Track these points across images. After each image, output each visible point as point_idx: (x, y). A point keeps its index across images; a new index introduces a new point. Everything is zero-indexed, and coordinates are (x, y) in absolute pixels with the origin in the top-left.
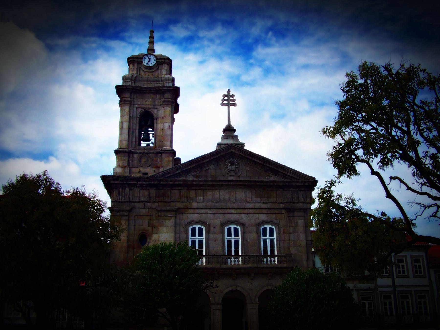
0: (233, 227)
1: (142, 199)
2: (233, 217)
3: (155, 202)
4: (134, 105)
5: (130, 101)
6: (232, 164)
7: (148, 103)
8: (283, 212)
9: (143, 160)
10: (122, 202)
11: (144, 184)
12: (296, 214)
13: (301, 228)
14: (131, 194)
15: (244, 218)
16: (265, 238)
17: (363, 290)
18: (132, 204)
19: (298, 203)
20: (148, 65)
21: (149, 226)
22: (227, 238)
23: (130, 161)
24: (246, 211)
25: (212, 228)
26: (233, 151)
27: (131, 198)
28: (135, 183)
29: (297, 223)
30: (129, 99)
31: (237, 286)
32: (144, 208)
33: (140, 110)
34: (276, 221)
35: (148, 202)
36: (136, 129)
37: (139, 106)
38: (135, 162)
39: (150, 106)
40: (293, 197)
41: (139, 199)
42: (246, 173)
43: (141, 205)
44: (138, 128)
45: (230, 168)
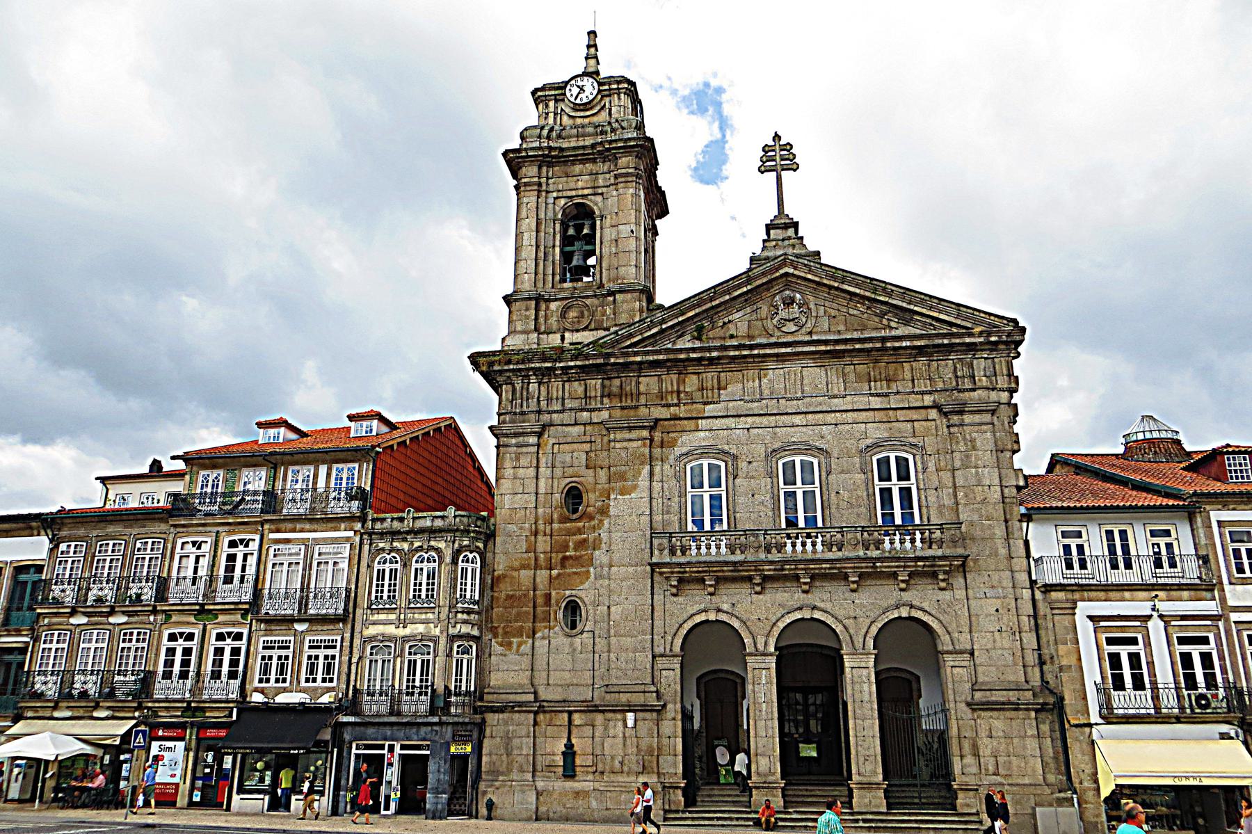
0: (798, 459)
1: (569, 404)
2: (797, 435)
3: (600, 410)
4: (548, 192)
5: (540, 184)
6: (789, 302)
7: (580, 184)
8: (933, 414)
9: (572, 314)
10: (523, 413)
11: (571, 368)
12: (968, 418)
13: (985, 455)
14: (544, 393)
15: (827, 437)
16: (885, 484)
17: (1184, 618)
18: (545, 418)
19: (974, 390)
20: (578, 101)
21: (587, 467)
22: (783, 488)
23: (542, 320)
24: (831, 418)
25: (743, 465)
26: (791, 271)
27: (543, 403)
28: (549, 365)
29: (973, 441)
30: (536, 179)
31: (814, 608)
32: (576, 424)
33: (563, 202)
34: (914, 441)
35: (582, 410)
36: (554, 246)
37: (560, 194)
38: (553, 321)
39: (586, 192)
40: (957, 377)
41: (563, 404)
42: (825, 321)
43: (567, 417)
44: (558, 243)
45: (783, 314)
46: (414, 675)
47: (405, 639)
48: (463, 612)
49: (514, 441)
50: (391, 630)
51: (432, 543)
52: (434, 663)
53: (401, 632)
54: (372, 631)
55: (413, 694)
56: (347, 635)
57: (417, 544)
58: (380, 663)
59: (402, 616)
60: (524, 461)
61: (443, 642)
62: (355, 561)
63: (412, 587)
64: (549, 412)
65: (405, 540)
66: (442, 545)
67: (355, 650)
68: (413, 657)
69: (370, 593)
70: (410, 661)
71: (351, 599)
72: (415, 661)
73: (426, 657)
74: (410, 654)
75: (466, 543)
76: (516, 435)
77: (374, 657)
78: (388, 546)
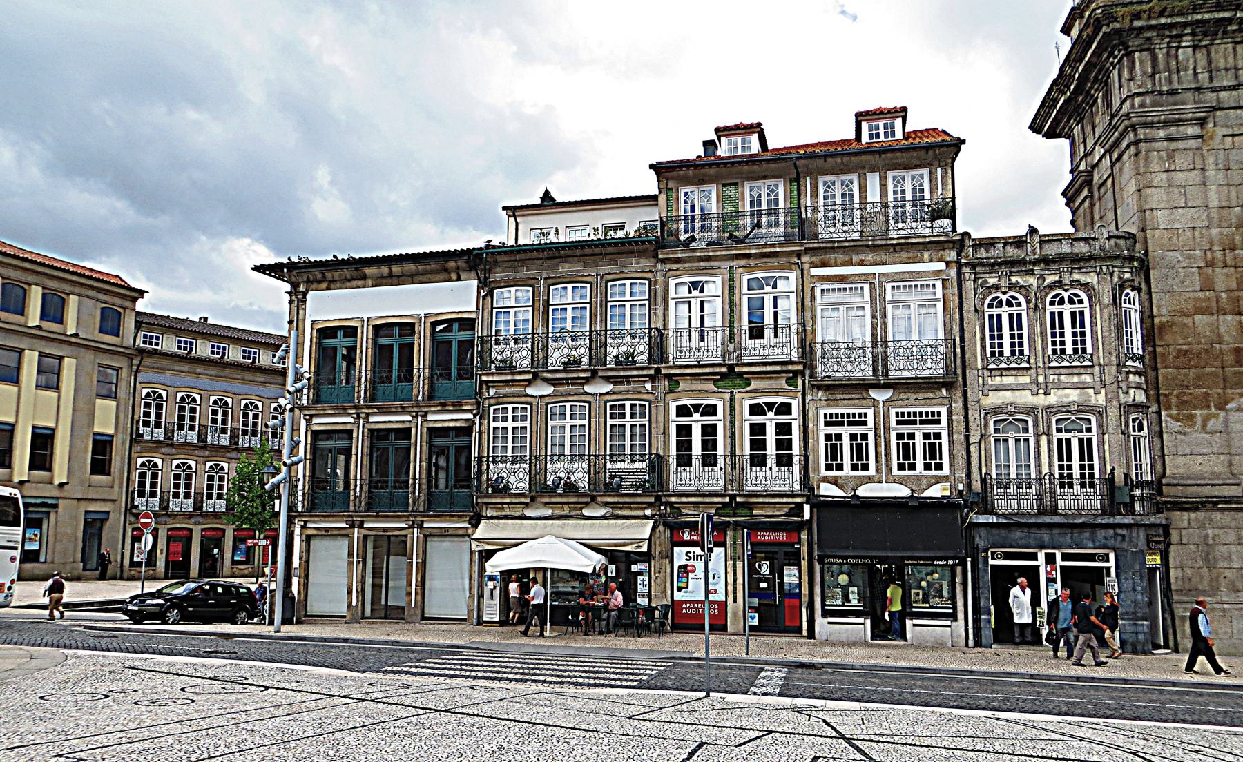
10: (1172, 92)
18: (1210, 98)
46: (1069, 459)
47: (1050, 410)
48: (1134, 373)
49: (1161, 134)
50: (1025, 398)
51: (1076, 277)
52: (1101, 443)
53: (1041, 400)
54: (994, 399)
55: (1071, 485)
56: (958, 406)
57: (1050, 279)
58: (1012, 443)
59: (1041, 379)
60: (1181, 161)
61: (1113, 413)
62: (955, 306)
63: (1049, 339)
64: (1214, 90)
65: (1030, 273)
66: (1092, 278)
67: (972, 426)
68: (1064, 435)
69: (983, 348)
70: (1060, 441)
71: (957, 359)
72: (1068, 441)
73: (1085, 435)
74: (1059, 430)
75: (1127, 276)
76: (1166, 124)
77: (1001, 436)
78: (1004, 282)
